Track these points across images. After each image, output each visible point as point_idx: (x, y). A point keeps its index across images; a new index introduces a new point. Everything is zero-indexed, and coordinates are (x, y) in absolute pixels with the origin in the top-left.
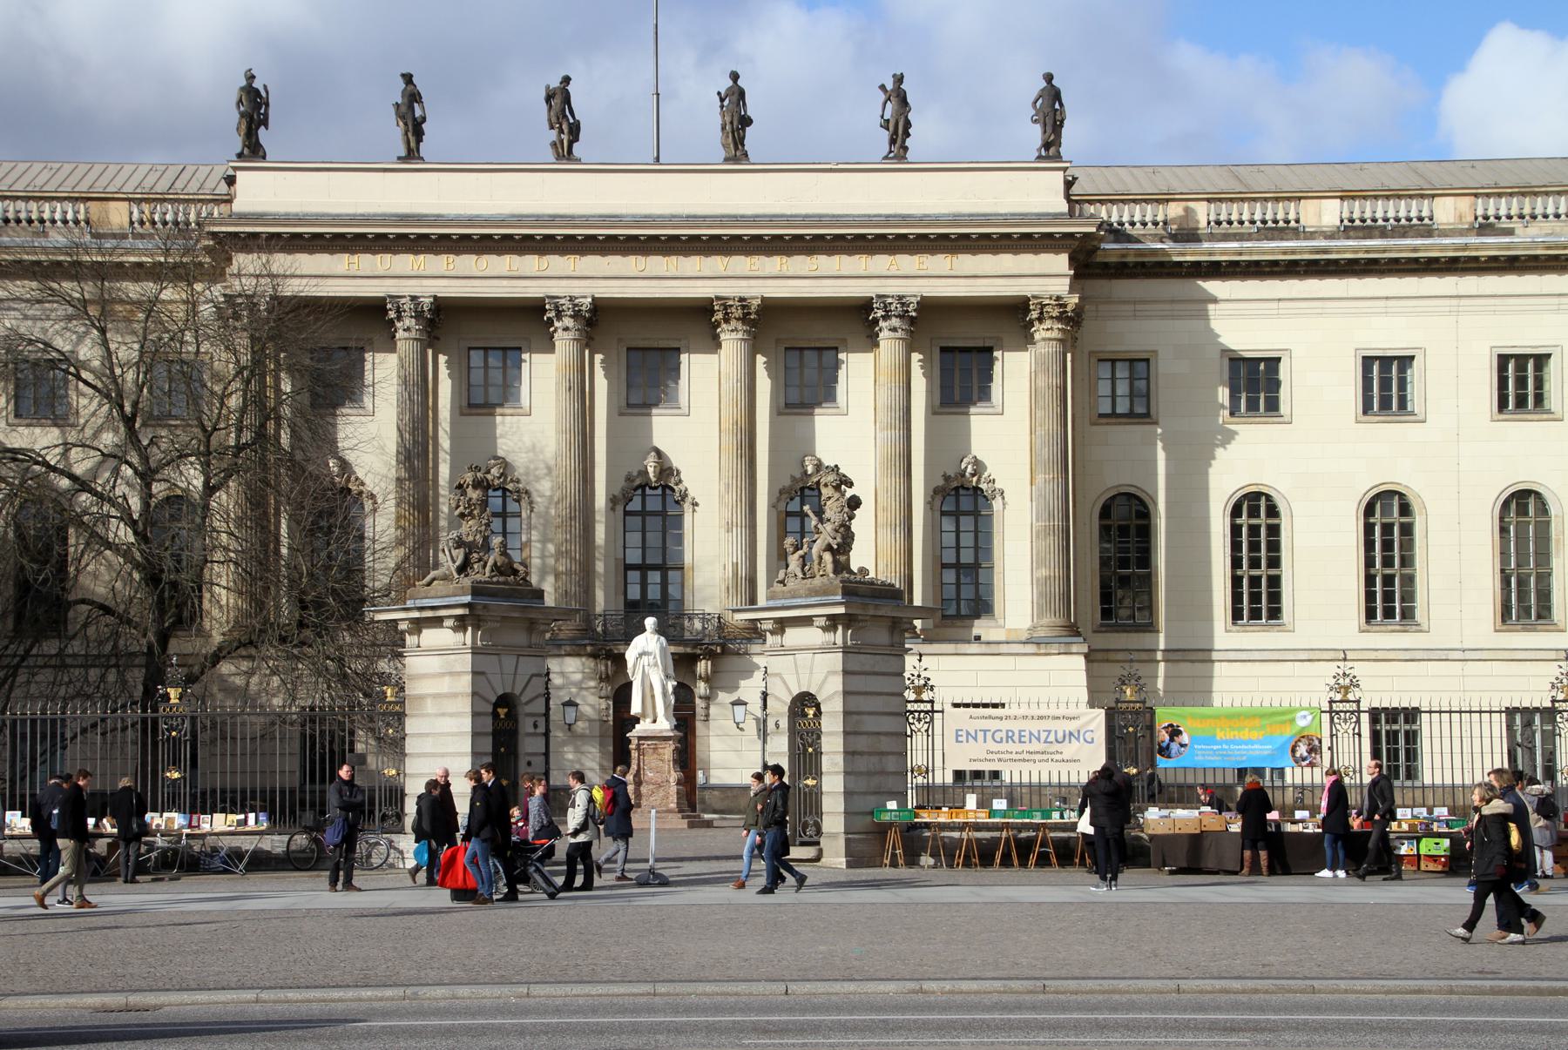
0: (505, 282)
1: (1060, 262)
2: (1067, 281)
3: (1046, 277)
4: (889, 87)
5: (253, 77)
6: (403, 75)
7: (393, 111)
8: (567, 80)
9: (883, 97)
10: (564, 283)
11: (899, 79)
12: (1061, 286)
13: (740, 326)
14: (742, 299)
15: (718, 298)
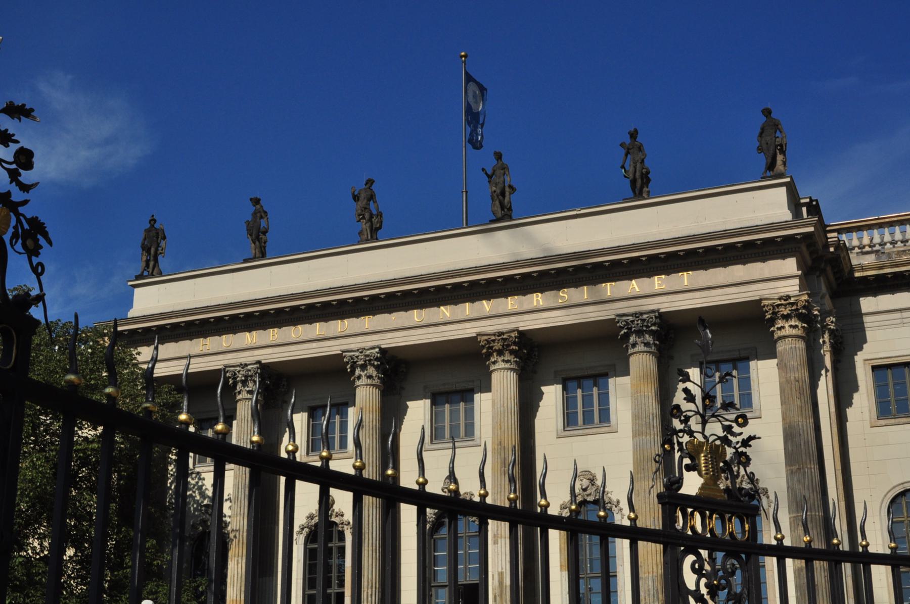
0: (314, 345)
1: (790, 265)
2: (797, 281)
3: (778, 280)
4: (628, 140)
5: (155, 221)
6: (251, 199)
7: (244, 227)
8: (370, 182)
9: (624, 152)
10: (359, 339)
11: (633, 135)
12: (792, 287)
13: (512, 358)
14: (501, 334)
15: (479, 334)
